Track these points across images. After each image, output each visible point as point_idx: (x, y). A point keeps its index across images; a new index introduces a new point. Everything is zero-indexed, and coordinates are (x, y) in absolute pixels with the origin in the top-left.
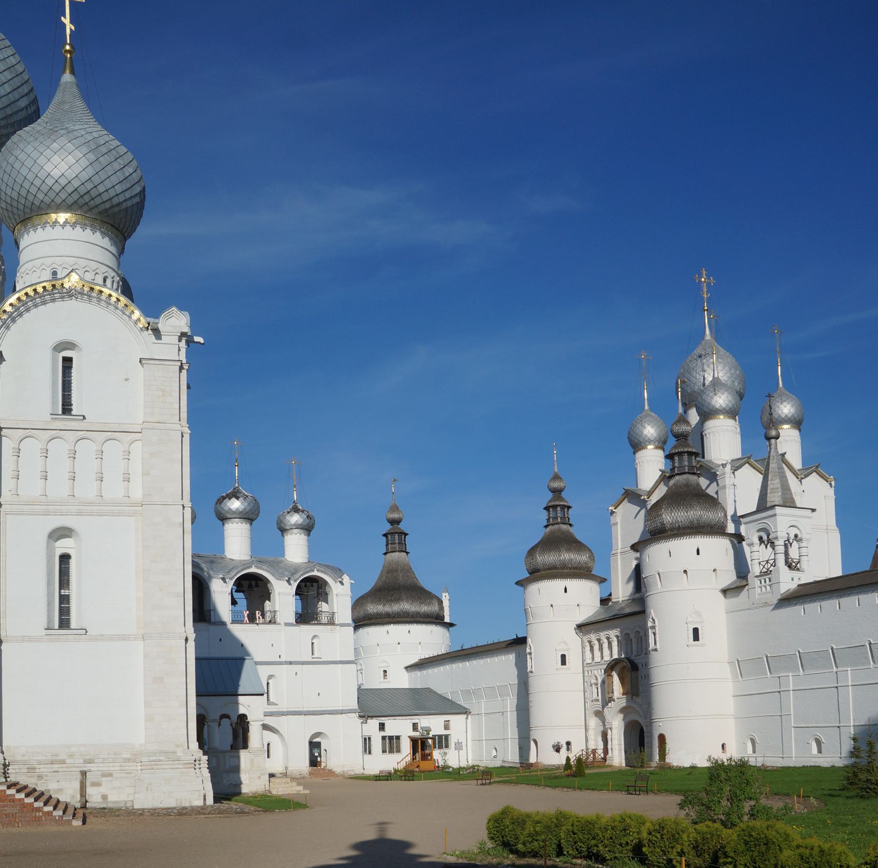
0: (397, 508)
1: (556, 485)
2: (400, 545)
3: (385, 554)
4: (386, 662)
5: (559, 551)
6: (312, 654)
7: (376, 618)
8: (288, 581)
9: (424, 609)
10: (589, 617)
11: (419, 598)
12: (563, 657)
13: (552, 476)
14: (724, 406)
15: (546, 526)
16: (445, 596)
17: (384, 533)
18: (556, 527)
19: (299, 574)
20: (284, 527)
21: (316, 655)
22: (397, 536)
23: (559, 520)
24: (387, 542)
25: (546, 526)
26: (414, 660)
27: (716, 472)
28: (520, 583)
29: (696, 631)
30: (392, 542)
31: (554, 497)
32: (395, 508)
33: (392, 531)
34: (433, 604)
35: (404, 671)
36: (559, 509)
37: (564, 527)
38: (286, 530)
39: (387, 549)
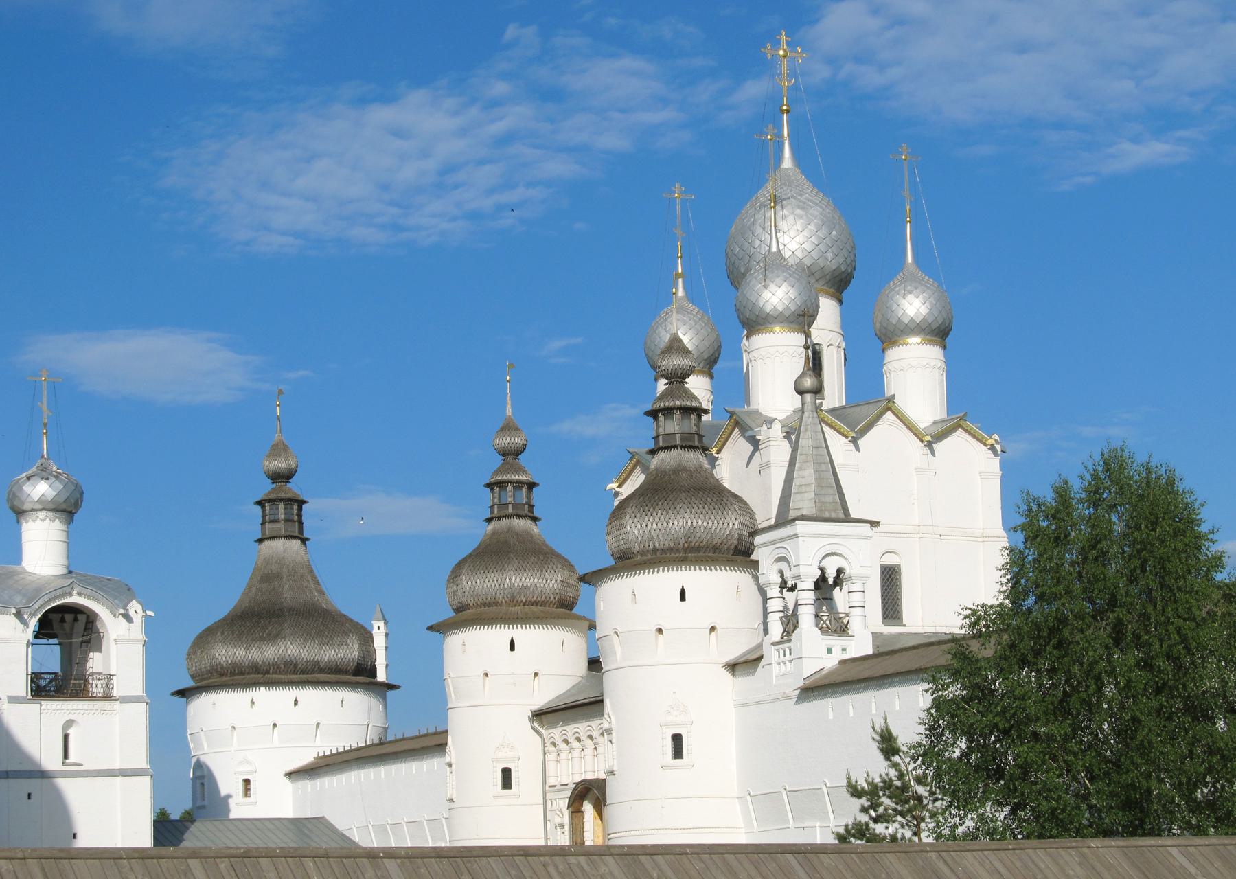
0: (285, 447)
1: (507, 441)
2: (290, 523)
3: (260, 541)
4: (249, 763)
5: (502, 570)
6: (66, 756)
7: (233, 674)
8: (19, 615)
9: (329, 654)
10: (558, 697)
11: (320, 634)
12: (506, 773)
13: (500, 424)
14: (780, 308)
15: (489, 520)
16: (379, 628)
17: (259, 499)
18: (504, 523)
19: (41, 602)
20: (20, 507)
21: (72, 759)
22: (281, 507)
23: (510, 510)
24: (264, 516)
25: (489, 520)
26: (305, 758)
27: (755, 436)
28: (442, 628)
29: (677, 739)
30: (272, 518)
31: (503, 464)
32: (279, 449)
33: (273, 496)
34: (347, 645)
35: (286, 780)
36: (510, 487)
37: (529, 522)
38: (24, 511)
39: (263, 532)
